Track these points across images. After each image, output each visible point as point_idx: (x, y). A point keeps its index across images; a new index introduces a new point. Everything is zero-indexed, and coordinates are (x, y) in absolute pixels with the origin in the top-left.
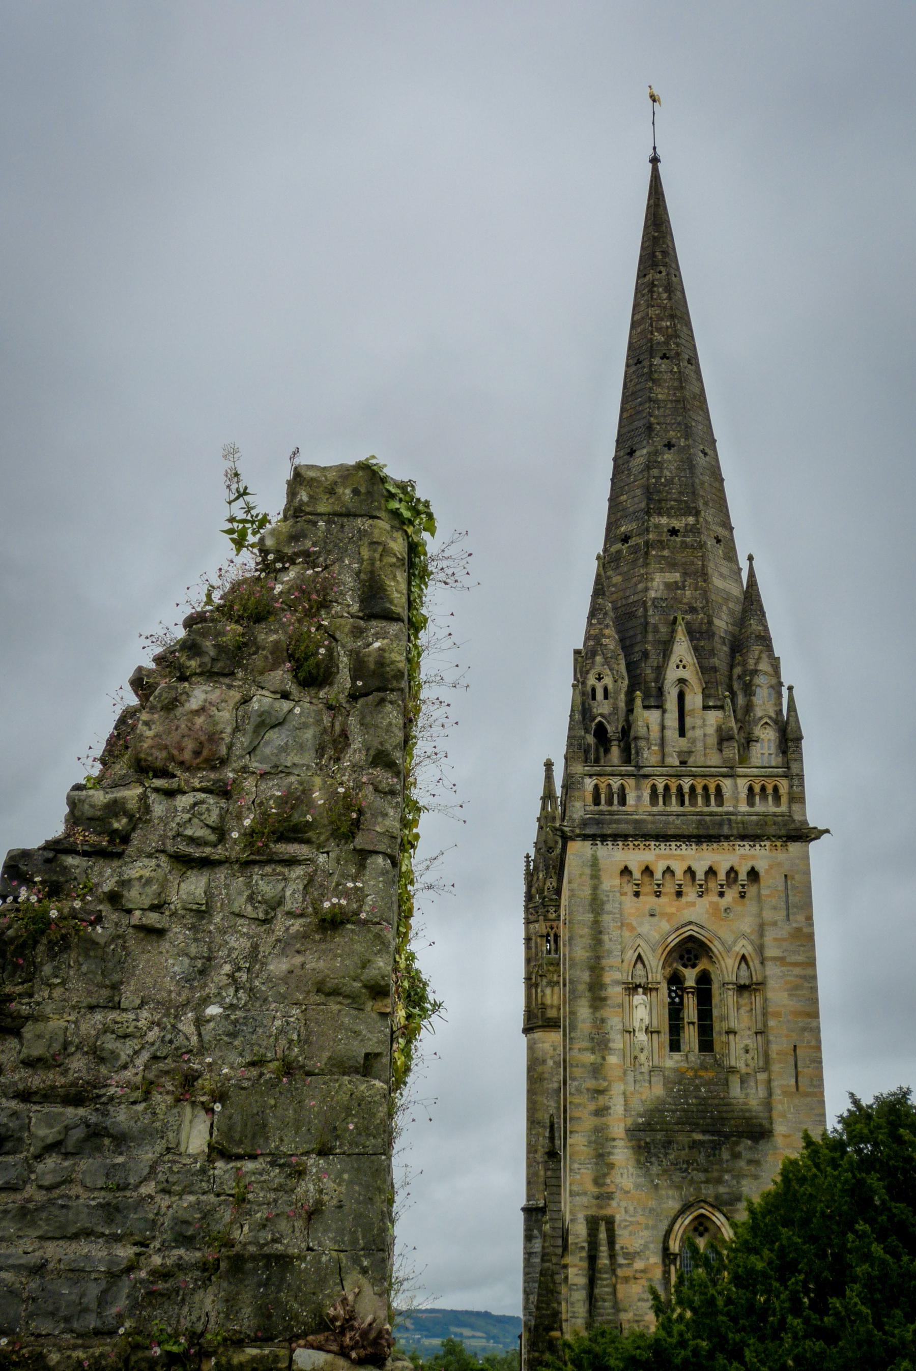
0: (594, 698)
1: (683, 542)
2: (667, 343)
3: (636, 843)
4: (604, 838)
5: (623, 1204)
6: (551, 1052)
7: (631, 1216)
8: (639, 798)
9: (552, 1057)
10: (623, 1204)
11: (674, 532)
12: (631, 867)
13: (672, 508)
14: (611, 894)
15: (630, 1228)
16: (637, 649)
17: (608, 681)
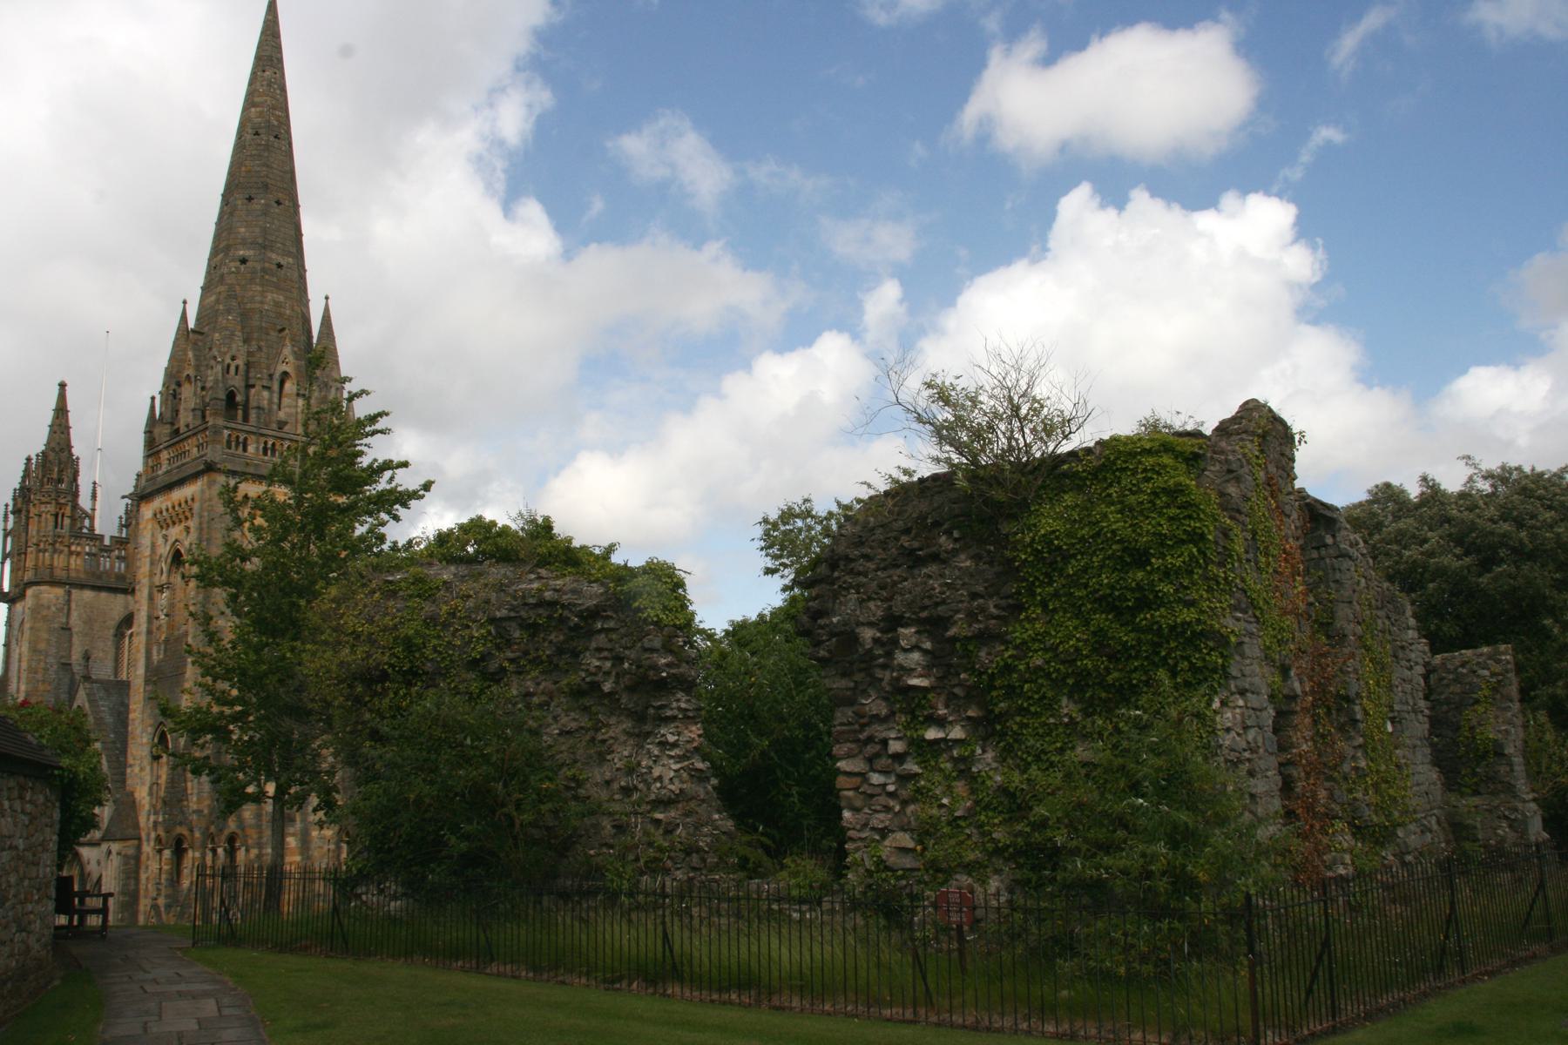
0: (228, 372)
8: (257, 448)
9: (55, 605)
11: (280, 266)
16: (254, 343)
17: (240, 362)
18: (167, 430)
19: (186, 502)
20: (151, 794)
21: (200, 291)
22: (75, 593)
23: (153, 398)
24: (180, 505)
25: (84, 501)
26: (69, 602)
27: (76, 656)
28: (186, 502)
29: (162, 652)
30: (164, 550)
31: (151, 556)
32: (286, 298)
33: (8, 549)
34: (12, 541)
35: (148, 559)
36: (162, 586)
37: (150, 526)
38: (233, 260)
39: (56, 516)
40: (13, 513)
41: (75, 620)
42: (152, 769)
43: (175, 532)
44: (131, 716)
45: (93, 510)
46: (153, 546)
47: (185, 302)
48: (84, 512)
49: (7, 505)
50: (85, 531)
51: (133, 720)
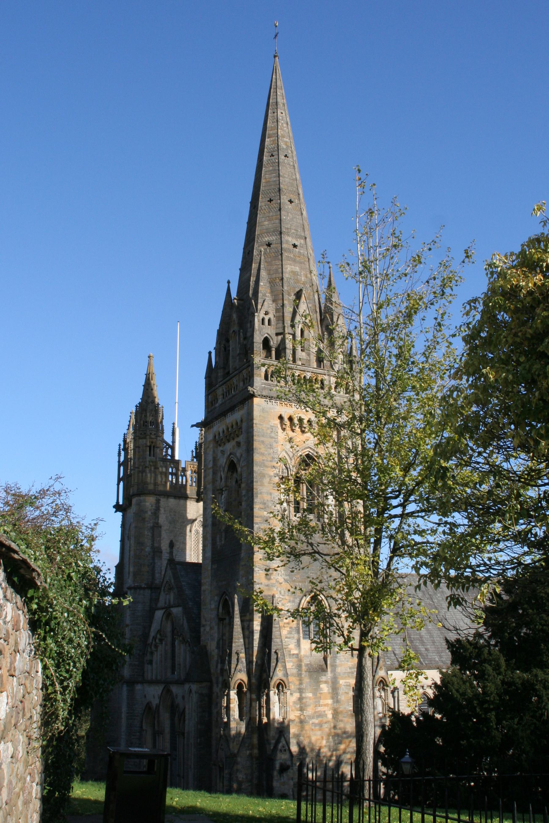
0: (263, 323)
1: (299, 252)
2: (287, 149)
3: (286, 403)
4: (271, 398)
5: (279, 589)
6: (150, 507)
7: (283, 596)
10: (279, 589)
11: (295, 246)
12: (283, 415)
13: (293, 233)
14: (274, 428)
15: (282, 602)
18: (221, 373)
19: (237, 423)
20: (218, 647)
21: (239, 272)
22: (163, 501)
23: (210, 353)
24: (232, 426)
25: (167, 437)
26: (157, 509)
27: (165, 546)
28: (237, 423)
29: (223, 539)
30: (223, 461)
31: (213, 467)
32: (301, 269)
33: (121, 475)
34: (124, 469)
35: (211, 470)
36: (222, 490)
37: (211, 446)
38: (262, 246)
39: (150, 447)
40: (123, 450)
41: (162, 519)
42: (218, 628)
43: (229, 447)
44: (203, 588)
45: (174, 442)
46: (215, 460)
47: (229, 282)
48: (167, 444)
49: (120, 445)
50: (169, 457)
51: (204, 591)
